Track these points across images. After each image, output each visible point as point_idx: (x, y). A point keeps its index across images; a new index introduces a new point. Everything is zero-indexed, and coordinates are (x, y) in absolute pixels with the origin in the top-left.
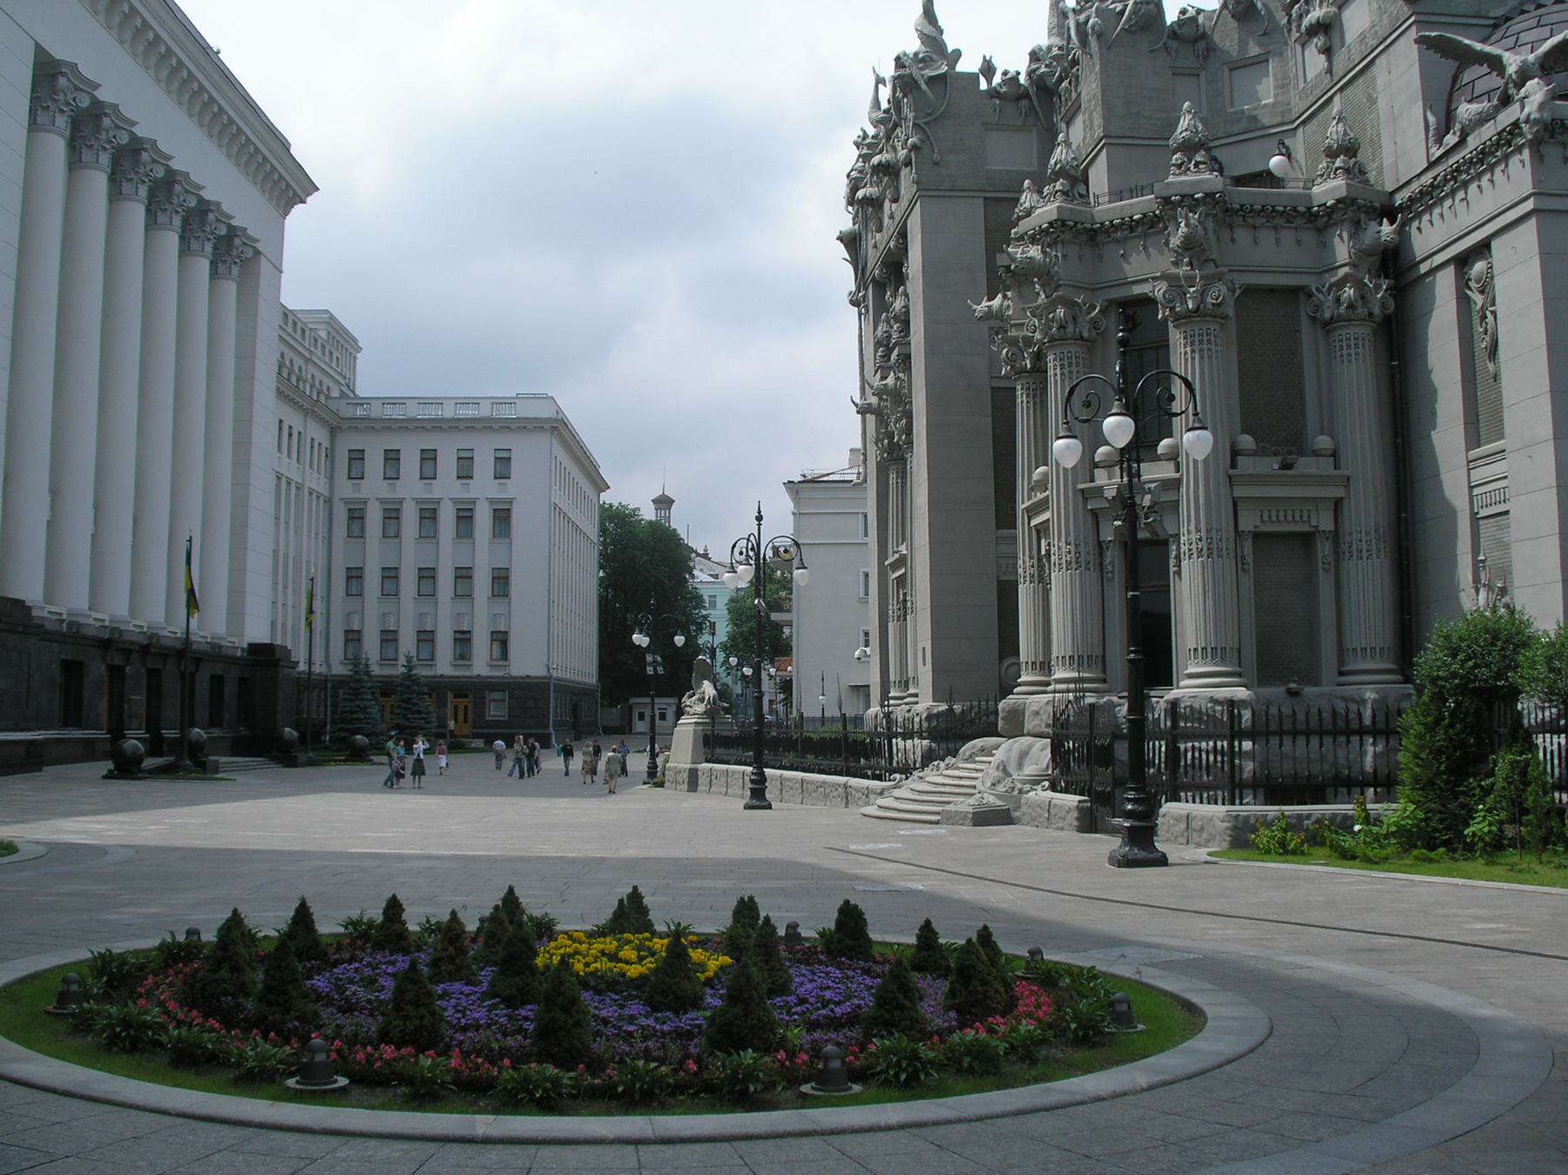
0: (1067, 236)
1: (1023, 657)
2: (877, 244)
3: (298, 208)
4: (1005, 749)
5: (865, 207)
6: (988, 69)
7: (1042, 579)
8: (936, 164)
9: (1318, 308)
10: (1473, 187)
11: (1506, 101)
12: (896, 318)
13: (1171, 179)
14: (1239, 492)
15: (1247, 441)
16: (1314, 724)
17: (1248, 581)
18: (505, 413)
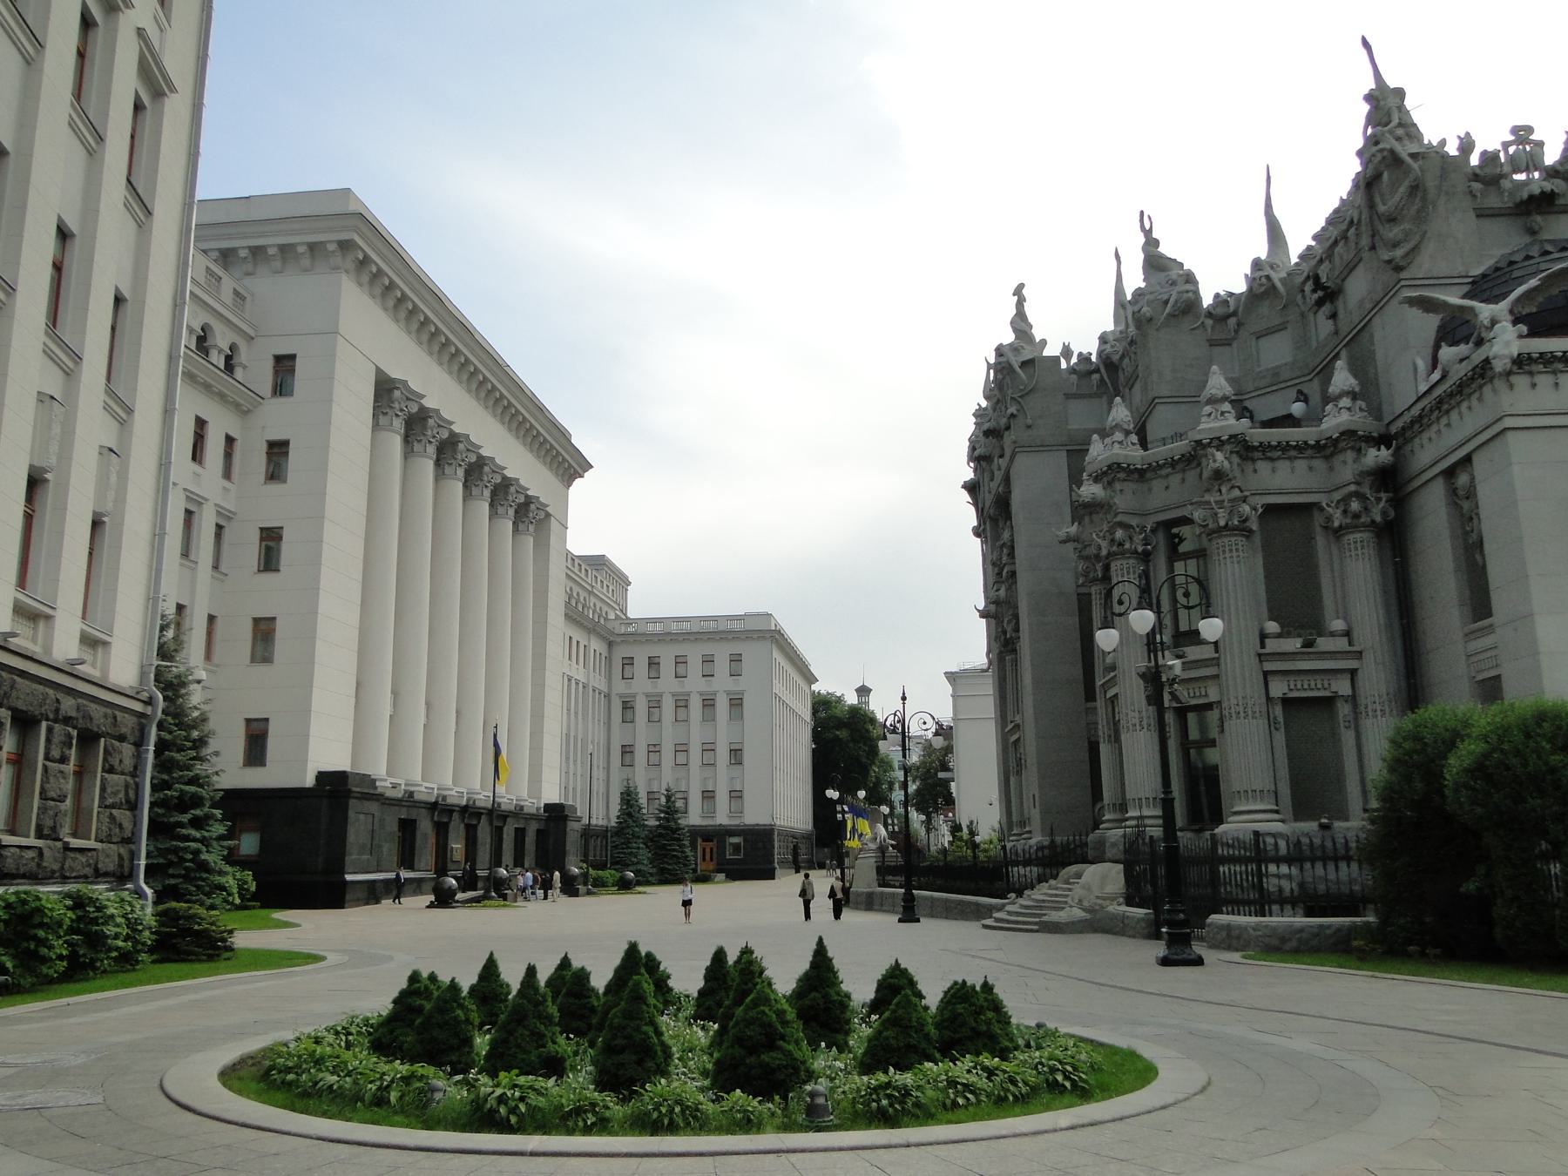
0: (1122, 475)
1: (1106, 801)
2: (992, 487)
3: (578, 481)
4: (1091, 872)
5: (979, 457)
6: (1067, 352)
7: (1116, 738)
8: (1029, 427)
9: (1329, 519)
10: (1454, 415)
11: (1480, 343)
13: (1202, 426)
14: (1268, 666)
15: (1272, 627)
16: (1342, 852)
17: (1280, 738)
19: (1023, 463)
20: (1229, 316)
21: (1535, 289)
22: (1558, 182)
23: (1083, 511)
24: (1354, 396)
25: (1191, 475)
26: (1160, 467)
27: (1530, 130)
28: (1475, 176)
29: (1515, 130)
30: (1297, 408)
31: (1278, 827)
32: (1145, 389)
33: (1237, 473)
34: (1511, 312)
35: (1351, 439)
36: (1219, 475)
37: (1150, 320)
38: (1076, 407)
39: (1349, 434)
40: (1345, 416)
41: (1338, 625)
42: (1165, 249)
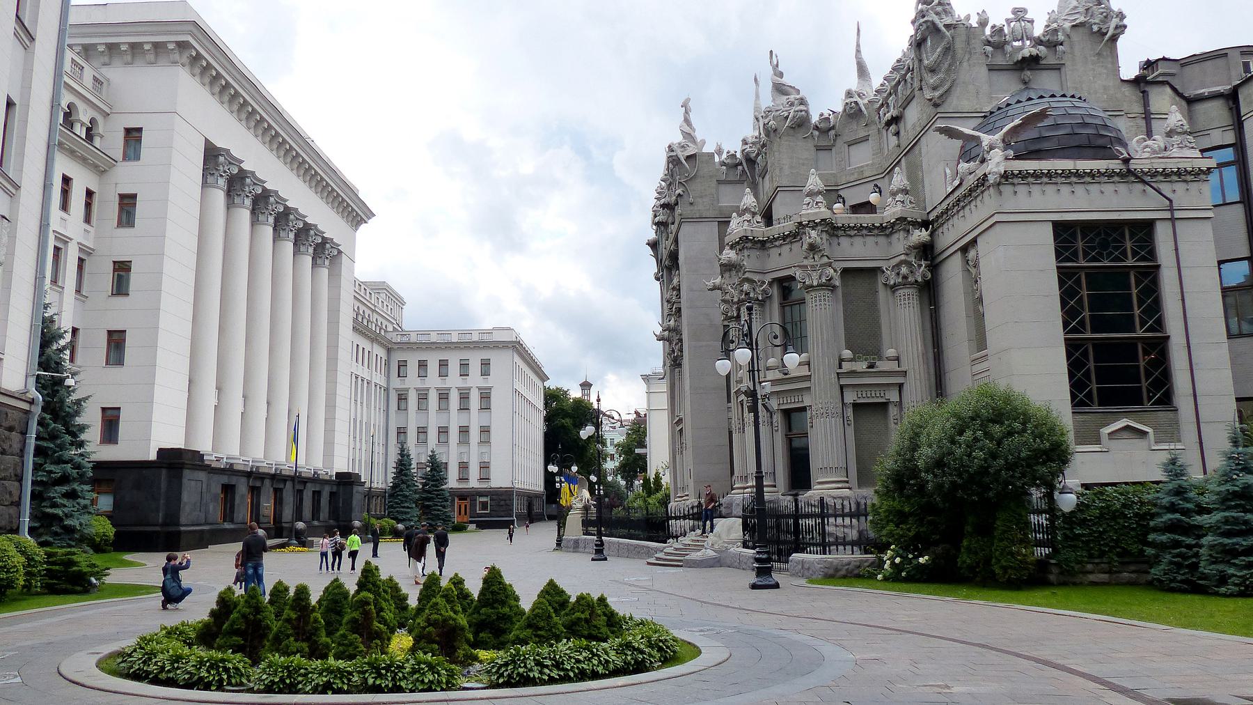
0: (749, 245)
1: (736, 474)
2: (666, 247)
3: (364, 226)
6: (720, 152)
10: (967, 208)
11: (983, 161)
12: (674, 289)
14: (843, 382)
15: (847, 353)
17: (850, 431)
18: (486, 338)
19: (686, 230)
20: (830, 129)
21: (1019, 125)
22: (1041, 48)
23: (728, 268)
24: (905, 192)
25: (796, 246)
26: (776, 239)
27: (1024, 11)
28: (989, 43)
29: (1016, 11)
30: (873, 198)
31: (846, 492)
32: (772, 180)
33: (826, 246)
34: (1003, 141)
35: (903, 224)
36: (813, 248)
37: (775, 131)
38: (726, 190)
39: (902, 220)
40: (899, 207)
41: (891, 352)
42: (786, 80)
